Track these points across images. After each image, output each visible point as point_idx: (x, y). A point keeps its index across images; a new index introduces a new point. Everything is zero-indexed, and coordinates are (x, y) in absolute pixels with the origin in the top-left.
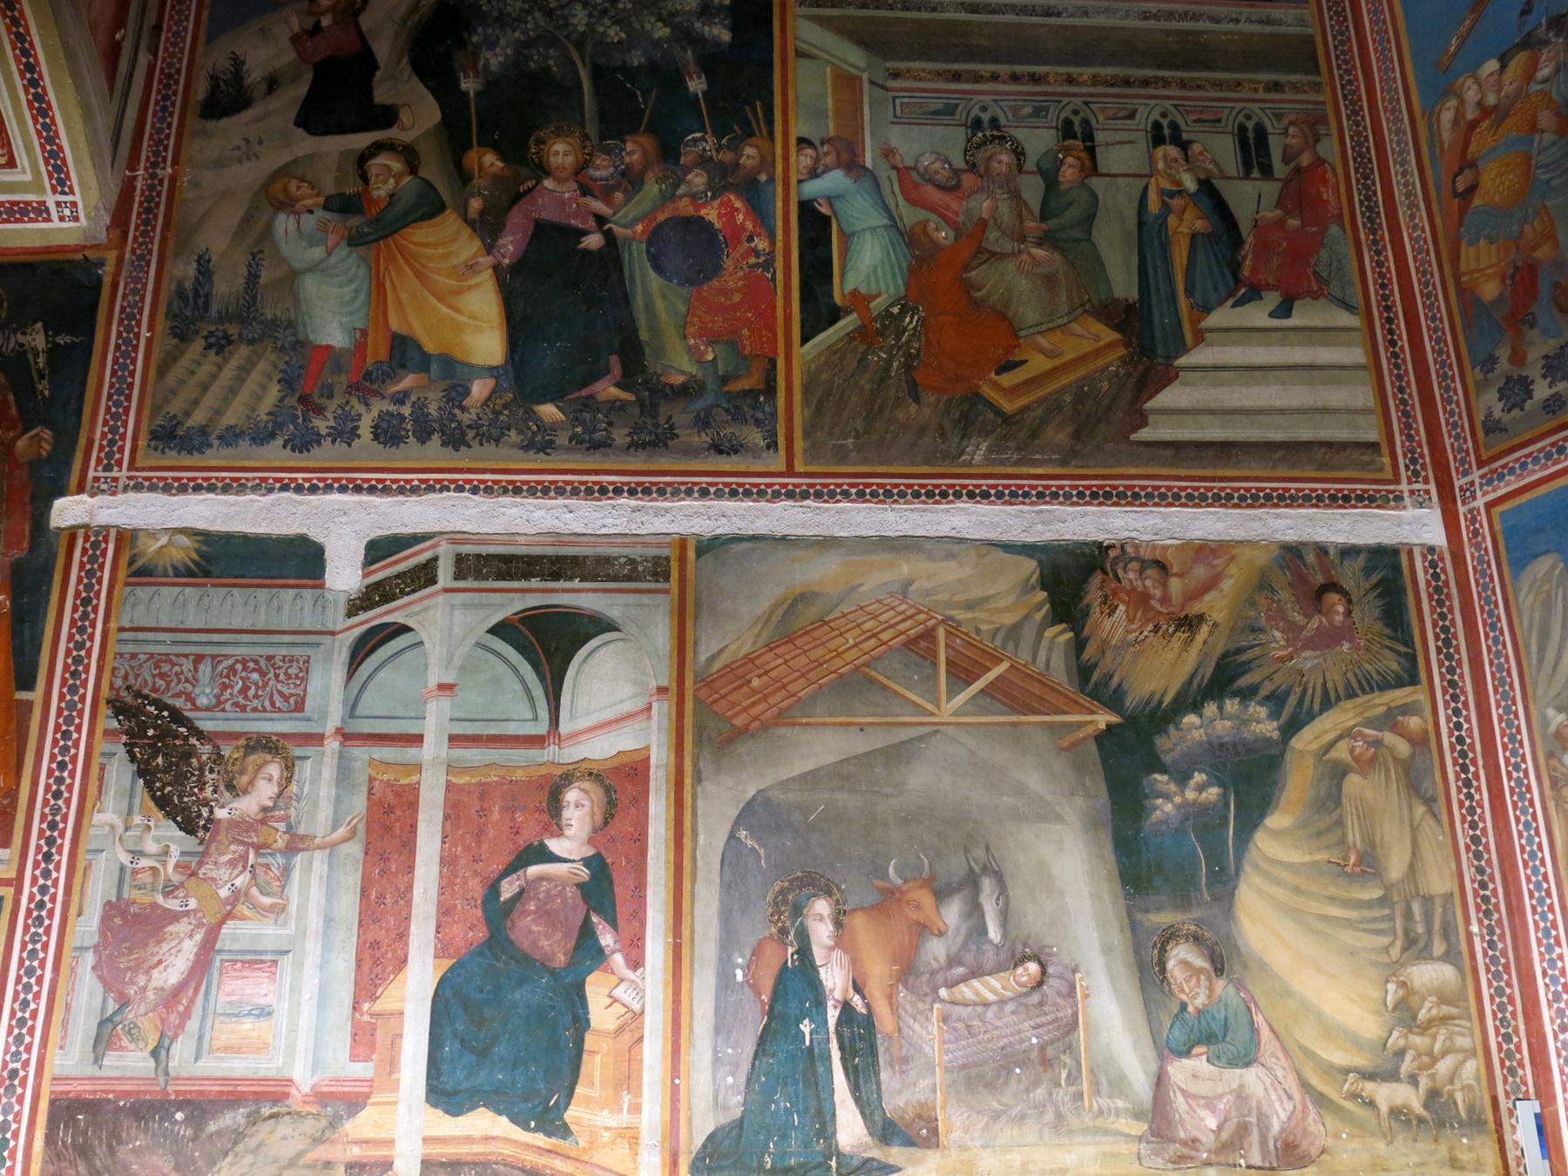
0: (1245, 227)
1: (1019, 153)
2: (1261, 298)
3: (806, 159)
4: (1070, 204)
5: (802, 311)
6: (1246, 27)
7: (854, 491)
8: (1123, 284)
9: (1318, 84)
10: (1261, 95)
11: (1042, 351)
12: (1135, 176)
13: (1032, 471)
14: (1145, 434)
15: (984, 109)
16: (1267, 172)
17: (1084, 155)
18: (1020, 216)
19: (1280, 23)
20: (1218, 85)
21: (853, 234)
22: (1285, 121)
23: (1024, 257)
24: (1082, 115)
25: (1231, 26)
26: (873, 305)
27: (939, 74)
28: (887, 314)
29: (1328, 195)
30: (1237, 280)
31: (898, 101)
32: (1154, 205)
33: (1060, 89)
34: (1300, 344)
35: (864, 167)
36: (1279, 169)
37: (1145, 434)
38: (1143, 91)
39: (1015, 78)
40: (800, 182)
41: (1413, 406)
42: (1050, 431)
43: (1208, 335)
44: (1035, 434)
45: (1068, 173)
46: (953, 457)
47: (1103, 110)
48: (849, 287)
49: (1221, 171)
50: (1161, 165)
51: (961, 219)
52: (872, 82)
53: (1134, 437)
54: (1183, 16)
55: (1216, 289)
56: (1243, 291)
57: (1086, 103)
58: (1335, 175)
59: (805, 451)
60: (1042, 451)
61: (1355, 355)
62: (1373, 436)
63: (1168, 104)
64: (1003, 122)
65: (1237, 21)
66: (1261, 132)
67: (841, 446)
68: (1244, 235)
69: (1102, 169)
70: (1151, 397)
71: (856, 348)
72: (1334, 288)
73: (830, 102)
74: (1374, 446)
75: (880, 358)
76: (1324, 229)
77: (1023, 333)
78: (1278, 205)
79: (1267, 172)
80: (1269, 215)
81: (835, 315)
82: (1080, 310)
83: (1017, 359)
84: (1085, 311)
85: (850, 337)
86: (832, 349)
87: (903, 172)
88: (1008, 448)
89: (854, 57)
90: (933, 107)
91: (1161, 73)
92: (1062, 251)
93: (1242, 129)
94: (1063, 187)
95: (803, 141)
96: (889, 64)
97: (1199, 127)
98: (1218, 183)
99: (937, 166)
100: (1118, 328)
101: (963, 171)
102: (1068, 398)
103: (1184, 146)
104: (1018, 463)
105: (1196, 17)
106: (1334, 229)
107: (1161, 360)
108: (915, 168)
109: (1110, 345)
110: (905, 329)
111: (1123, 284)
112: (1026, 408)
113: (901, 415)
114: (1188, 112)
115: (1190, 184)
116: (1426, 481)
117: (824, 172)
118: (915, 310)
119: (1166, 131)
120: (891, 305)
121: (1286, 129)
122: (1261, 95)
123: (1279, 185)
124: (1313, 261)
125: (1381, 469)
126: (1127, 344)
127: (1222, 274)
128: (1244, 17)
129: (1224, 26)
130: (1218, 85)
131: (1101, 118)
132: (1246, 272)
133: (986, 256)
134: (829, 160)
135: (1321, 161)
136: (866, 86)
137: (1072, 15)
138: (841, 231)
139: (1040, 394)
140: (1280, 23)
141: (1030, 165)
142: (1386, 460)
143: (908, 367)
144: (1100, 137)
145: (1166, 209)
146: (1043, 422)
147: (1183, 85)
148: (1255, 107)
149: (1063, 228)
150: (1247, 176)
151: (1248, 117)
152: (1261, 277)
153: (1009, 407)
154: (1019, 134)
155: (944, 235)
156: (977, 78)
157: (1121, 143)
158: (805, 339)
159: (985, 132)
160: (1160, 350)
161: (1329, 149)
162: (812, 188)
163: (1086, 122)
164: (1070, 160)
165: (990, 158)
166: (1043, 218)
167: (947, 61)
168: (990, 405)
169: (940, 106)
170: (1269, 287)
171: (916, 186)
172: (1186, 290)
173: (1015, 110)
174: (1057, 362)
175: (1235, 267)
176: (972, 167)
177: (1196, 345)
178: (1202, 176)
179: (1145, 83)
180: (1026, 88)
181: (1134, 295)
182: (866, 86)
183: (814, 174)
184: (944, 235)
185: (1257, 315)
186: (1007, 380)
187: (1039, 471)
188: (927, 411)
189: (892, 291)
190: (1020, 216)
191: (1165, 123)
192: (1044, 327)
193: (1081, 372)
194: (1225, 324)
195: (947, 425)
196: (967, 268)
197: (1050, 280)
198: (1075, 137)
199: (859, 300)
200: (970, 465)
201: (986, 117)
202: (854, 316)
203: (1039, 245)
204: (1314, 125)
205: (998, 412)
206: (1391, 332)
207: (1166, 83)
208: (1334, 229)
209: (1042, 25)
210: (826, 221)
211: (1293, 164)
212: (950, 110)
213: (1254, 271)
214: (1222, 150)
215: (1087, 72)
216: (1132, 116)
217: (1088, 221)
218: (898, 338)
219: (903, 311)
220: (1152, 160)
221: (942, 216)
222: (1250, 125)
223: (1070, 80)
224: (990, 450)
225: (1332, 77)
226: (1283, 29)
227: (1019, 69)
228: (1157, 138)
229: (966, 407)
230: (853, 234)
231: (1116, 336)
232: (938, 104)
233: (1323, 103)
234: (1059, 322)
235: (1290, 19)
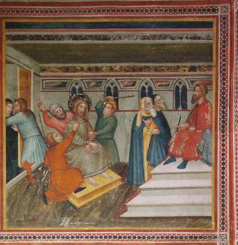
0: (173, 131)
1: (89, 103)
2: (175, 161)
3: (7, 109)
4: (106, 124)
5: (7, 170)
6: (185, 41)
7: (23, 236)
8: (124, 158)
9: (211, 66)
10: (187, 73)
11: (91, 184)
12: (132, 111)
13: (85, 229)
14: (126, 215)
15: (77, 84)
16: (185, 108)
17: (113, 103)
18: (87, 130)
19: (199, 38)
20: (169, 69)
21: (26, 139)
22: (195, 84)
23: (88, 146)
24: (114, 85)
25: (179, 41)
26: (32, 167)
27: (60, 68)
28: (37, 170)
29: (207, 116)
30: (167, 153)
31: (44, 82)
32: (138, 124)
33: (107, 74)
34: (188, 179)
35: (30, 111)
36: (190, 106)
37: (126, 215)
38: (139, 73)
39: (90, 69)
40: (7, 118)
41: (226, 203)
42: (92, 213)
43: (153, 176)
44: (87, 214)
45: (107, 111)
46: (57, 225)
47: (122, 82)
48: (24, 160)
49: (166, 107)
50: (143, 106)
51: (66, 131)
52: (35, 74)
53: (122, 216)
54: (160, 37)
55: (159, 157)
56: (169, 158)
57: (116, 80)
58: (212, 107)
59: (7, 222)
60: (89, 221)
61: (209, 182)
62: (210, 213)
63: (148, 79)
64: (84, 89)
65: (182, 38)
66: (185, 89)
67: (20, 221)
68: (172, 135)
69: (120, 109)
70: (129, 200)
71: (25, 184)
72: (204, 156)
73: (18, 84)
74: (209, 218)
75: (34, 188)
76: (204, 131)
77: (85, 177)
78: (188, 121)
79: (185, 108)
80: (183, 126)
81: (19, 171)
82: (107, 167)
83: (82, 187)
84: (109, 168)
85: (23, 180)
86: (18, 184)
87: (45, 113)
88: (77, 220)
89: (26, 61)
90: (55, 84)
91: (147, 64)
92: (102, 144)
93: (177, 88)
94: (104, 117)
95: (8, 100)
96: (41, 65)
97: (161, 88)
98: (165, 113)
99: (58, 109)
100: (120, 174)
101: (67, 111)
102: (100, 202)
103: (153, 97)
104: (81, 226)
105: (165, 37)
106: (208, 131)
107: (135, 186)
108: (49, 111)
109: (115, 182)
110: (43, 176)
111: (124, 158)
112: (85, 205)
113: (40, 209)
114: (156, 82)
115: (154, 114)
116: (226, 231)
117: (15, 113)
118: (47, 169)
119: (147, 91)
120: (39, 167)
121: (195, 88)
122: (187, 73)
123: (189, 112)
124: (197, 145)
125: (210, 227)
126: (122, 180)
127: (161, 150)
128: (185, 36)
129: (176, 41)
130: (169, 69)
131: (122, 86)
132: (171, 150)
133: (74, 147)
134: (17, 108)
135: (206, 101)
136: (32, 75)
137: (114, 39)
138: (22, 138)
139: (90, 200)
140: (199, 38)
141: (93, 108)
142: (213, 223)
143: (43, 190)
144: (120, 94)
145: (143, 125)
146: (91, 209)
147: (156, 69)
148: (183, 78)
149: (103, 134)
150: (176, 110)
151: (180, 83)
152: (176, 152)
153: (78, 205)
154: (90, 95)
155: (58, 138)
156: (75, 70)
157: (129, 97)
158: (8, 181)
159: (78, 94)
160: (135, 182)
161: (211, 97)
162: (11, 120)
163: (116, 88)
164: (108, 105)
165: (79, 104)
166: (96, 130)
167: (64, 63)
168: (71, 204)
169: (60, 83)
170: (178, 156)
171: (49, 117)
172: (147, 158)
173: (88, 83)
174: (97, 188)
175: (167, 148)
176: (71, 109)
177: (148, 180)
178: (159, 110)
179: (141, 69)
180: (93, 74)
181: (127, 161)
182: (32, 75)
183: (12, 115)
184: (58, 138)
185: (173, 167)
186: (79, 195)
187: (87, 229)
188: (49, 207)
189: (39, 162)
190: (87, 130)
191: (146, 87)
192: (93, 174)
193: (105, 191)
194: (160, 172)
195: (56, 212)
196: (66, 151)
197: (97, 155)
198: (111, 95)
199: (27, 165)
200: (63, 227)
201: (77, 87)
202: (25, 171)
203: (93, 141)
204: (206, 86)
205: (74, 207)
206: (223, 173)
207: (148, 69)
208: (208, 131)
209: (102, 44)
210: (16, 133)
211: (195, 103)
212: (63, 85)
213: (174, 150)
214: (167, 98)
215: (117, 66)
216: (134, 85)
217: (113, 130)
218: (40, 180)
219: (43, 169)
220: (140, 104)
221: (58, 130)
222: (180, 87)
223: (111, 69)
224: (71, 221)
225: (217, 63)
226: (200, 41)
227: (92, 65)
228: (143, 95)
229: (63, 205)
230: (26, 139)
231: (119, 177)
232: (58, 82)
233: (211, 75)
234: (99, 172)
235: (204, 36)
